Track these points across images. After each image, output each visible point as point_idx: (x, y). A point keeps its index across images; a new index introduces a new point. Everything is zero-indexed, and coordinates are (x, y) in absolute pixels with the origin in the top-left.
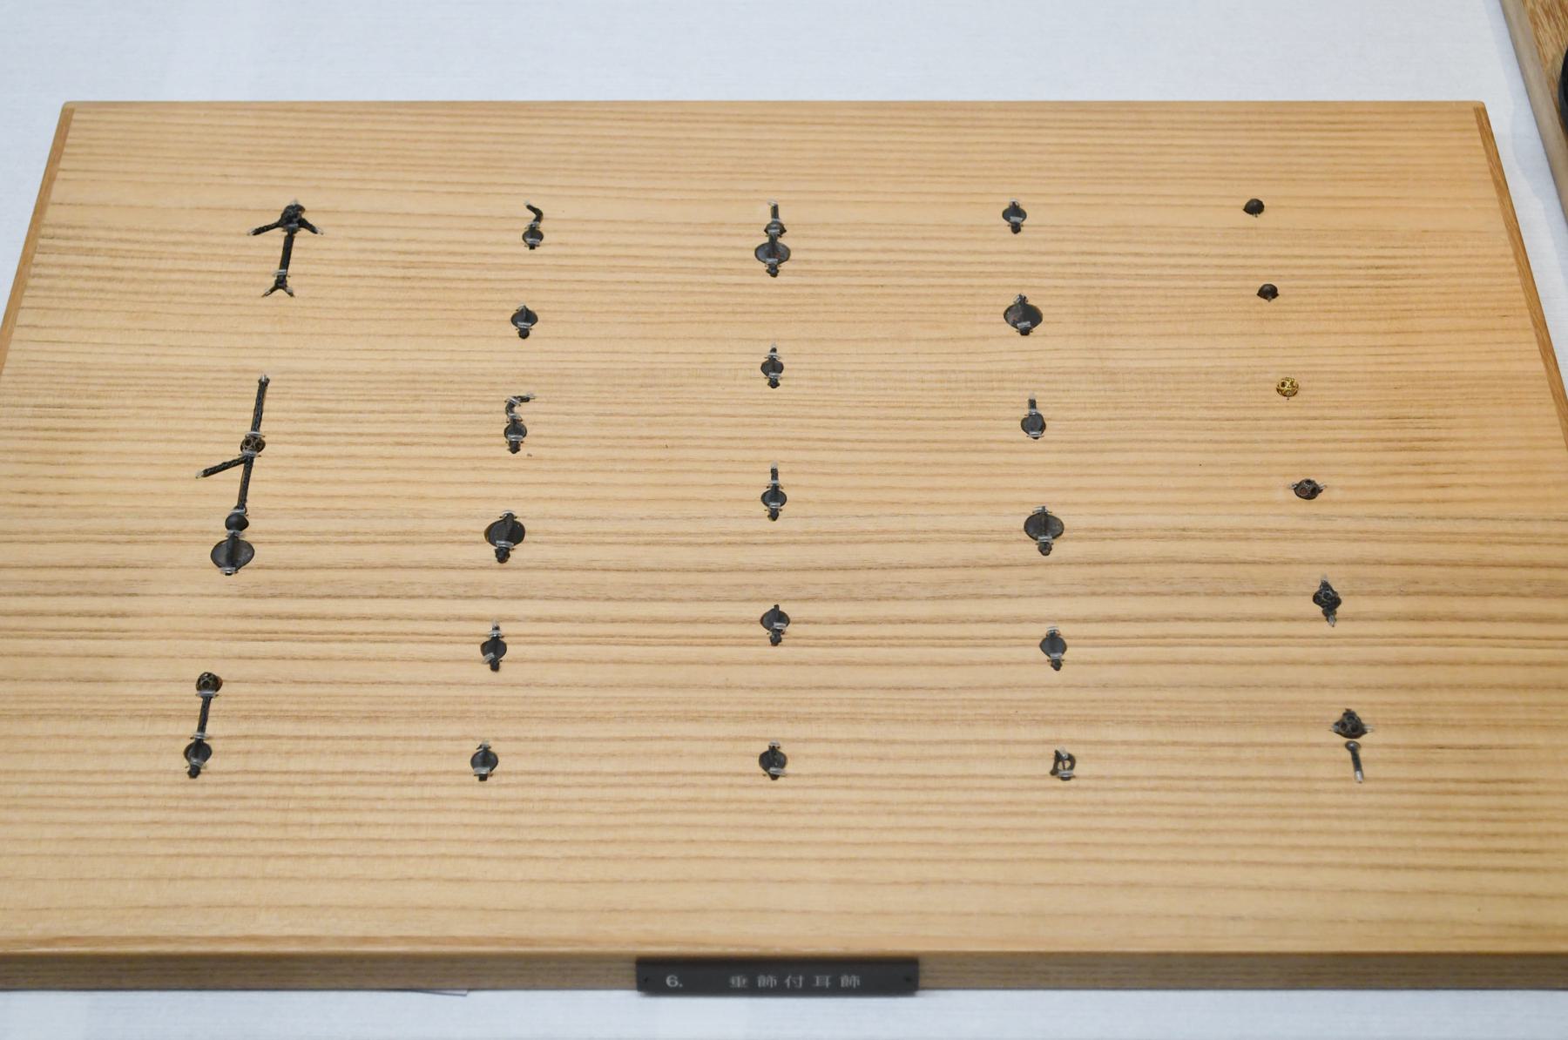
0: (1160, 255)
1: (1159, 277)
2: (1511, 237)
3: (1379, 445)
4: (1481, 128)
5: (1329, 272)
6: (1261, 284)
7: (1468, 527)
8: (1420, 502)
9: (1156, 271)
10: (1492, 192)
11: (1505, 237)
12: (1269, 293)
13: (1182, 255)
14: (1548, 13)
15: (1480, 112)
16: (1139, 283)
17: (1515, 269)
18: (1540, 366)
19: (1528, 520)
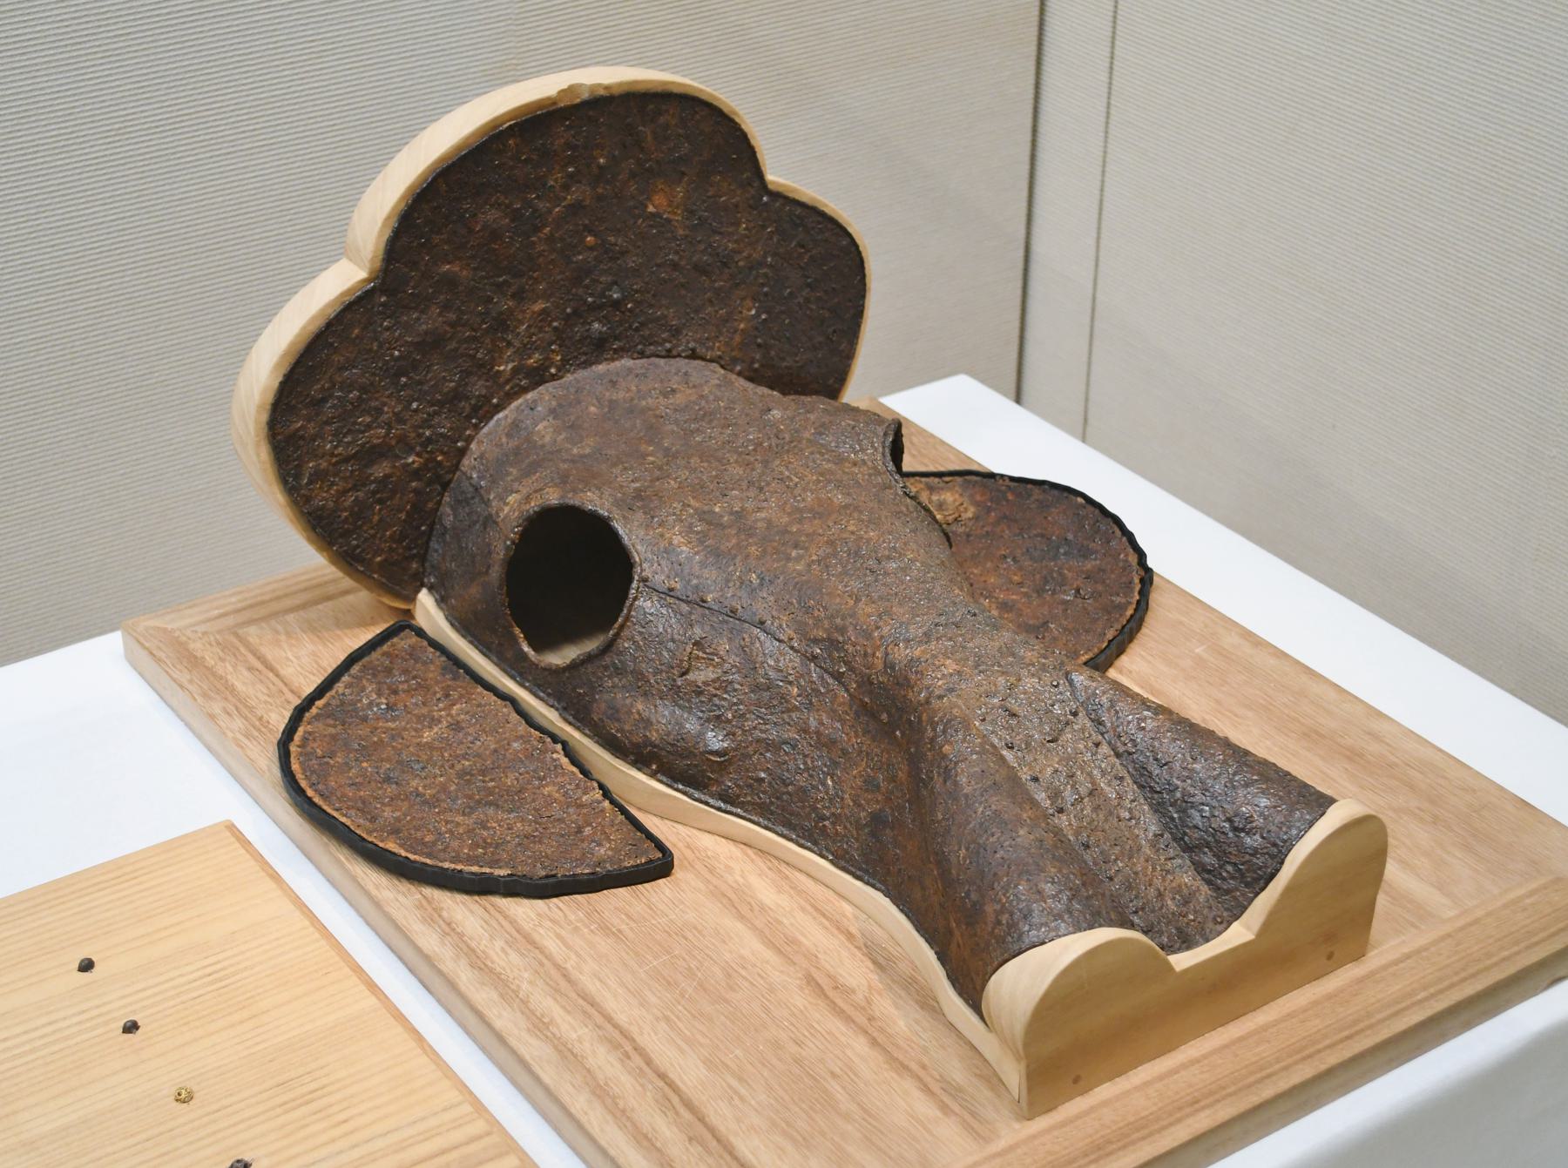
0: (25, 1032)
1: (32, 1051)
2: (303, 913)
3: (279, 1110)
4: (238, 839)
5: (172, 993)
6: (122, 1024)
7: (380, 1143)
8: (333, 1140)
9: (27, 1047)
10: (271, 885)
11: (298, 913)
12: (131, 1027)
13: (44, 1026)
14: (247, 736)
15: (231, 828)
16: (17, 1062)
17: (317, 935)
18: (373, 1000)
19: (423, 1119)
